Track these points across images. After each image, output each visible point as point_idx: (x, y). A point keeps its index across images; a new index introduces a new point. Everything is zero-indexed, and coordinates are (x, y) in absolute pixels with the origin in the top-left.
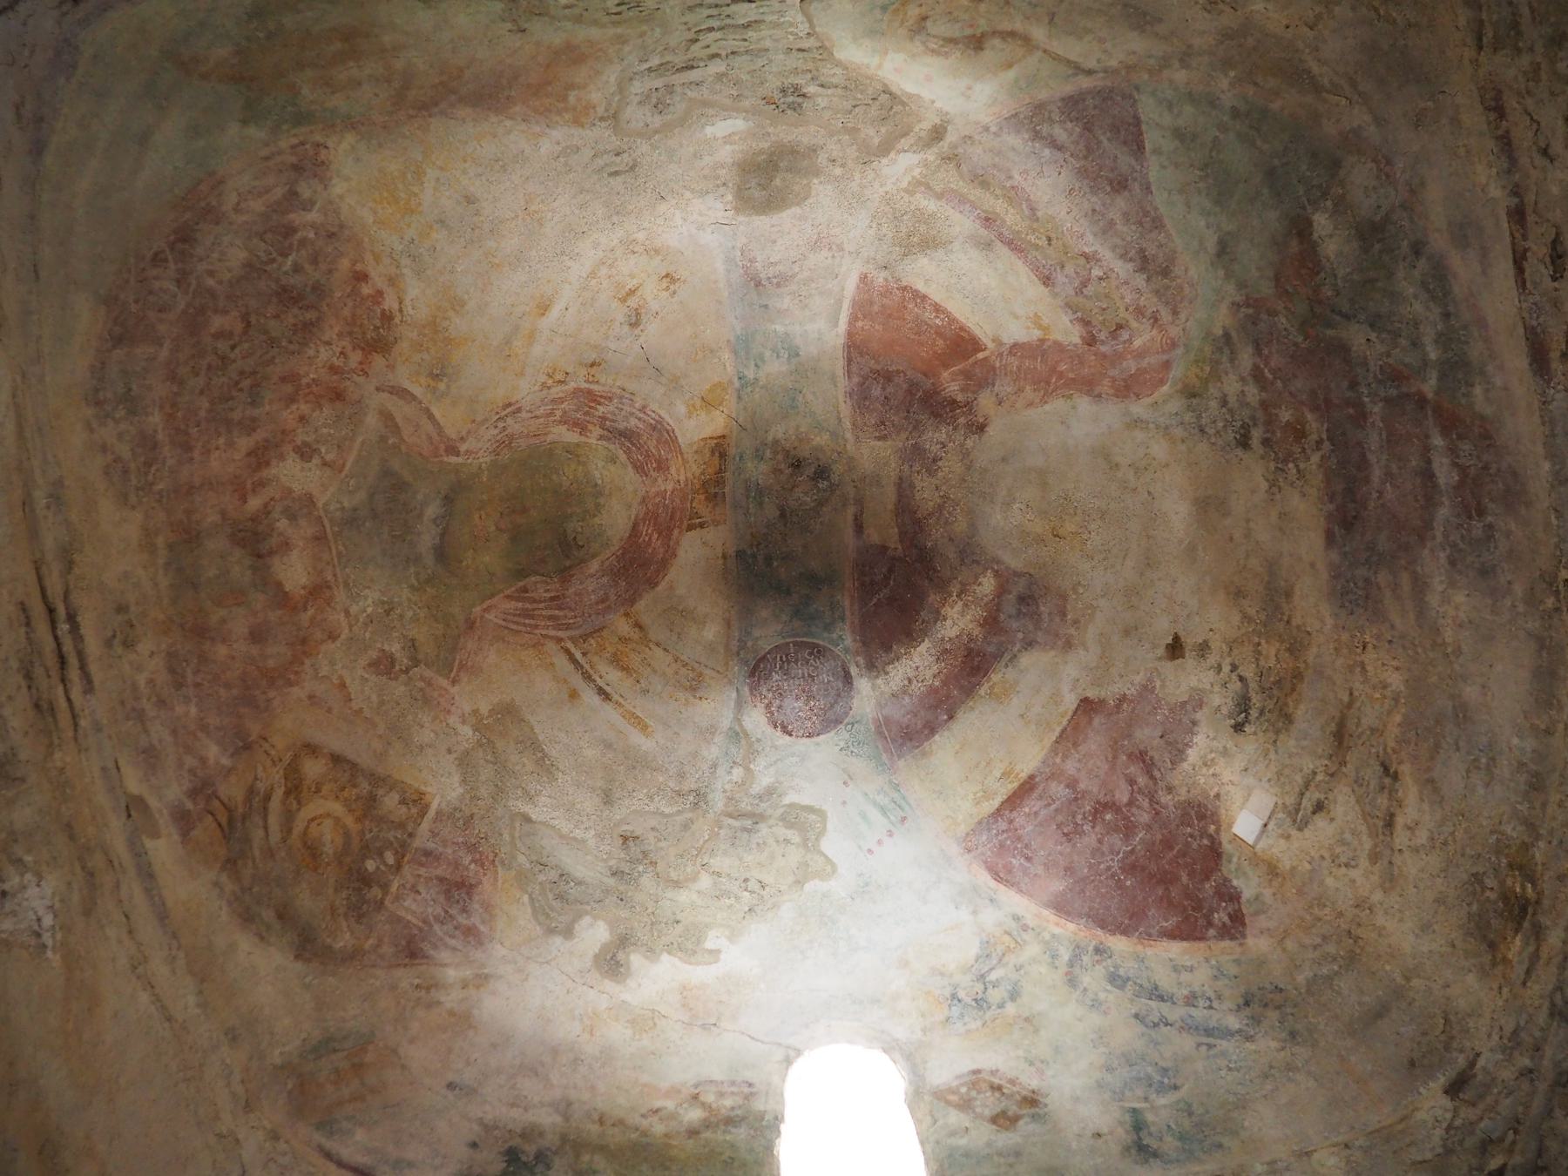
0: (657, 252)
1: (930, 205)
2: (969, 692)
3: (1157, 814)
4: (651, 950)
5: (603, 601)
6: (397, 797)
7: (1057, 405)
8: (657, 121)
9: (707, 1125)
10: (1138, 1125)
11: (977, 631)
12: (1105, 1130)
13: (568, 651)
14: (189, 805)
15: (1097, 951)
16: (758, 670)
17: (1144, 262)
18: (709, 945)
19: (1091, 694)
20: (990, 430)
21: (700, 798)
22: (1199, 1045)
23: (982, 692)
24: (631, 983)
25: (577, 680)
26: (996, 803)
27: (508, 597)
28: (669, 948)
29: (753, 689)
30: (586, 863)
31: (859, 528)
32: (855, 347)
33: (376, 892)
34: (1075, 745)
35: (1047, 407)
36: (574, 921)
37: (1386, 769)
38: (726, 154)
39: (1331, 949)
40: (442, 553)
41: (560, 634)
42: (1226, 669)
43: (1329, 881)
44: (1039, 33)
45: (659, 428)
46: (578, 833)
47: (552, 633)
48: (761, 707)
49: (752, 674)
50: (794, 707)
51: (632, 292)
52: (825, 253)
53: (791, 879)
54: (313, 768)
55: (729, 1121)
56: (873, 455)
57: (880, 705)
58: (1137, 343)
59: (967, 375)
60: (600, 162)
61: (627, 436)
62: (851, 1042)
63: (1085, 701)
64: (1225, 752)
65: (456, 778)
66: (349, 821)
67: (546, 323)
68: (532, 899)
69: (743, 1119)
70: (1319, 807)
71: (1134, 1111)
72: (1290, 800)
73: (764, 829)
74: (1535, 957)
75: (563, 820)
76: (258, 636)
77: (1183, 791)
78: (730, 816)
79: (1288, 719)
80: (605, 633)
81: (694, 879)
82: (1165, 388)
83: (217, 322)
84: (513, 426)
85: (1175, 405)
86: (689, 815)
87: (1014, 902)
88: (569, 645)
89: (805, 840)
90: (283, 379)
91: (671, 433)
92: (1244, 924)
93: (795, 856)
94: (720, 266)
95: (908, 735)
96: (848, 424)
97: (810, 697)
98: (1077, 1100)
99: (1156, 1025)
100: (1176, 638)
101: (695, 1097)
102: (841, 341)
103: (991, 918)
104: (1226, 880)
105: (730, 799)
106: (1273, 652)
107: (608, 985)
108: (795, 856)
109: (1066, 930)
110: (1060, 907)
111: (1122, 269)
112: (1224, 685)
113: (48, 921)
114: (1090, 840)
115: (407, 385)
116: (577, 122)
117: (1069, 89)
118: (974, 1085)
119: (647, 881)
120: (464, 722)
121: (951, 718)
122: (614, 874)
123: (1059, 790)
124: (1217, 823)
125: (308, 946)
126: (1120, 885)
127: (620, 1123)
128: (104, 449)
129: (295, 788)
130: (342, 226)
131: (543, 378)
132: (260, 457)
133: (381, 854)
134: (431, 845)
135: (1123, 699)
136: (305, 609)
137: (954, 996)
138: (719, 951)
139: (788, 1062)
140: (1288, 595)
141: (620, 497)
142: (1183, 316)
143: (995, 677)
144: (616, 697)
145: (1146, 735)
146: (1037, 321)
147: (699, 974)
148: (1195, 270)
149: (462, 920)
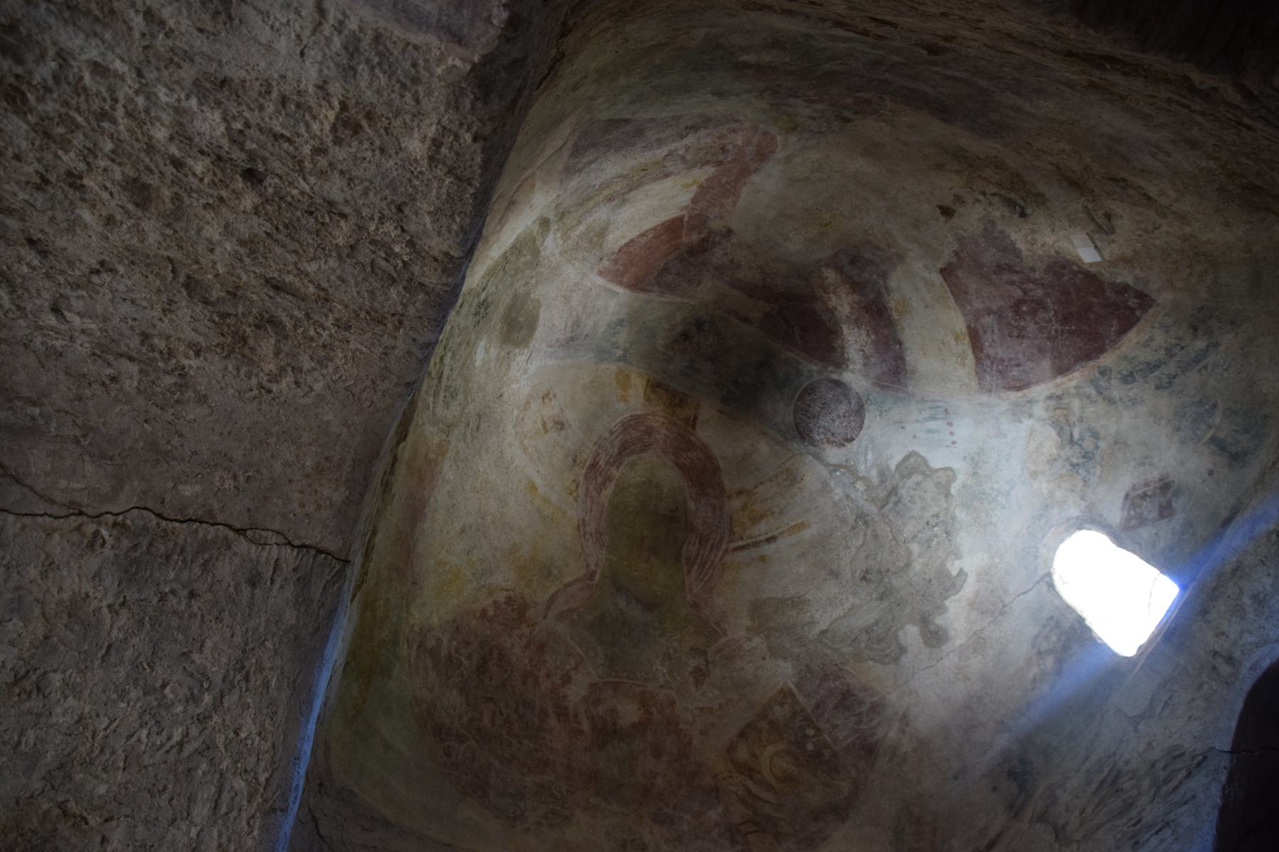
0: (528, 402)
1: (582, 228)
2: (891, 324)
3: (1042, 285)
4: (939, 608)
5: (715, 508)
6: (777, 708)
7: (745, 192)
8: (460, 397)
10: (1219, 445)
11: (856, 297)
12: (1211, 466)
13: (736, 549)
16: (802, 433)
17: (694, 128)
18: (954, 572)
21: (862, 517)
22: (1199, 371)
24: (952, 633)
25: (755, 552)
26: (971, 356)
27: (689, 572)
28: (944, 597)
29: (813, 443)
30: (869, 614)
31: (746, 320)
32: (637, 285)
33: (827, 752)
34: (966, 293)
35: (743, 196)
38: (493, 352)
40: (649, 607)
41: (723, 547)
42: (981, 198)
43: (1157, 242)
44: (527, 173)
45: (627, 426)
47: (721, 553)
50: (838, 426)
51: (544, 424)
52: (574, 295)
53: (942, 497)
54: (742, 754)
56: (705, 291)
57: (866, 376)
58: (740, 143)
59: (692, 228)
60: (469, 436)
61: (624, 448)
62: (1062, 541)
64: (1033, 232)
65: (781, 663)
67: (541, 490)
68: (873, 659)
70: (1108, 216)
72: (1092, 226)
73: (903, 492)
75: (835, 610)
76: (657, 753)
77: (1039, 264)
79: (1039, 195)
81: (910, 553)
82: (779, 138)
83: (486, 721)
84: (591, 528)
85: (793, 139)
86: (869, 531)
87: (1040, 391)
88: (733, 545)
90: (524, 683)
91: (632, 418)
92: (1147, 296)
93: (929, 485)
94: (551, 362)
95: (895, 372)
96: (679, 299)
98: (1182, 463)
99: (1170, 383)
100: (941, 208)
101: (1039, 653)
102: (628, 292)
103: (1039, 410)
104: (1113, 284)
105: (873, 500)
107: (946, 648)
108: (929, 485)
109: (1074, 379)
110: (1061, 370)
111: (690, 140)
112: (991, 204)
114: (1032, 327)
115: (547, 597)
116: (444, 454)
117: (566, 153)
118: (1134, 506)
119: (896, 582)
120: (751, 640)
121: (900, 343)
122: (882, 599)
123: (989, 320)
124: (1073, 263)
125: (839, 811)
126: (1073, 333)
128: (539, 824)
129: (748, 770)
130: (454, 621)
131: (571, 498)
132: (562, 713)
133: (806, 736)
134: (813, 702)
135: (956, 254)
136: (651, 714)
137: (1073, 465)
138: (961, 570)
139: (1051, 585)
141: (657, 469)
142: (742, 118)
143: (892, 304)
144: (776, 533)
145: (990, 256)
146: (687, 186)
147: (969, 588)
148: (719, 108)
149: (864, 708)
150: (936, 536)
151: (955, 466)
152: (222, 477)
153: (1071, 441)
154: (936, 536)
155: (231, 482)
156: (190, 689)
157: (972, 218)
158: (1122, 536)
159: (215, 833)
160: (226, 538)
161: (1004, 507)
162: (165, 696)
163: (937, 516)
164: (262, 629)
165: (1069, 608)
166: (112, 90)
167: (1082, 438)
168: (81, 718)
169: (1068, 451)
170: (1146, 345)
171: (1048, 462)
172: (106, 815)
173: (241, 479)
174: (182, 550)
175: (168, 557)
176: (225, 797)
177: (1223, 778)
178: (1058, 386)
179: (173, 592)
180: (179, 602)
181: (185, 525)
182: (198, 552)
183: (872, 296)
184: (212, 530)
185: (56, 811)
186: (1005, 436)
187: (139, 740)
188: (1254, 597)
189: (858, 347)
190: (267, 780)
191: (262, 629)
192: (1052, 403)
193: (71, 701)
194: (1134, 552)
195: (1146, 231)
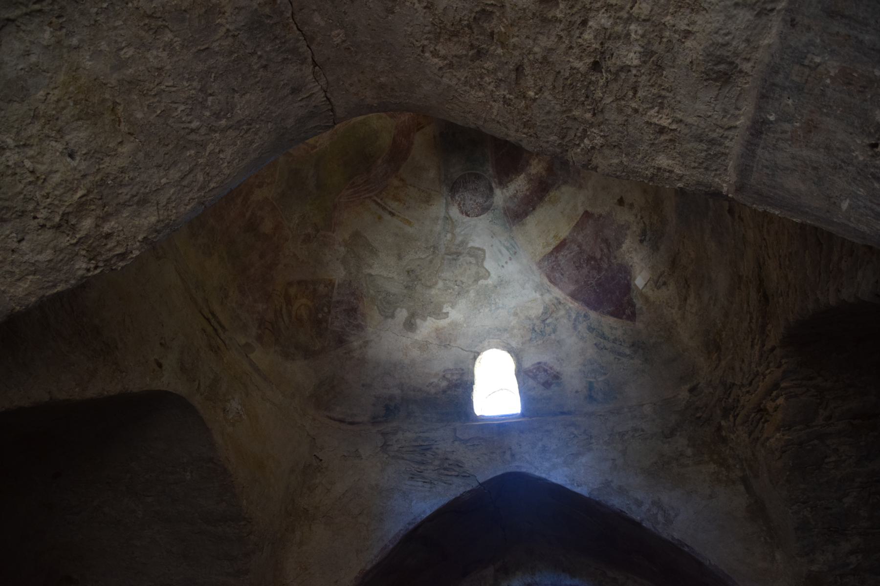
2: (541, 199)
9: (449, 388)
10: (590, 387)
11: (544, 173)
13: (375, 201)
14: (260, 332)
16: (454, 188)
18: (444, 311)
19: (589, 209)
24: (418, 332)
26: (551, 248)
28: (430, 315)
29: (453, 197)
30: (395, 288)
42: (639, 217)
46: (390, 275)
47: (367, 195)
48: (456, 205)
49: (451, 191)
54: (293, 291)
55: (456, 386)
62: (497, 348)
63: (586, 212)
64: (636, 250)
70: (665, 284)
71: (591, 383)
73: (461, 258)
75: (384, 272)
78: (447, 254)
81: (436, 283)
87: (557, 293)
88: (375, 198)
89: (477, 262)
95: (517, 215)
100: (622, 198)
101: (444, 376)
103: (547, 297)
107: (410, 334)
109: (573, 305)
110: (574, 296)
112: (638, 223)
113: (240, 408)
114: (585, 271)
118: (538, 369)
119: (419, 288)
121: (534, 209)
127: (420, 390)
135: (600, 216)
137: (533, 329)
139: (475, 358)
143: (552, 194)
144: (397, 213)
147: (443, 323)
151: (492, 275)
152: (339, 35)
153: (544, 321)
155: (339, 41)
156: (221, 110)
157: (624, 216)
158: (521, 373)
159: (172, 191)
160: (306, 58)
162: (206, 100)
163: (463, 283)
164: (274, 115)
167: (548, 325)
168: (159, 69)
169: (537, 322)
170: (611, 328)
172: (131, 131)
173: (345, 45)
174: (284, 43)
175: (276, 38)
176: (190, 178)
177: (468, 489)
178: (565, 299)
180: (256, 63)
181: (298, 32)
183: (550, 182)
184: (306, 48)
185: (110, 104)
186: (524, 288)
187: (176, 109)
188: (544, 446)
189: (518, 188)
190: (213, 188)
191: (274, 115)
192: (555, 301)
193: (164, 55)
195: (667, 303)
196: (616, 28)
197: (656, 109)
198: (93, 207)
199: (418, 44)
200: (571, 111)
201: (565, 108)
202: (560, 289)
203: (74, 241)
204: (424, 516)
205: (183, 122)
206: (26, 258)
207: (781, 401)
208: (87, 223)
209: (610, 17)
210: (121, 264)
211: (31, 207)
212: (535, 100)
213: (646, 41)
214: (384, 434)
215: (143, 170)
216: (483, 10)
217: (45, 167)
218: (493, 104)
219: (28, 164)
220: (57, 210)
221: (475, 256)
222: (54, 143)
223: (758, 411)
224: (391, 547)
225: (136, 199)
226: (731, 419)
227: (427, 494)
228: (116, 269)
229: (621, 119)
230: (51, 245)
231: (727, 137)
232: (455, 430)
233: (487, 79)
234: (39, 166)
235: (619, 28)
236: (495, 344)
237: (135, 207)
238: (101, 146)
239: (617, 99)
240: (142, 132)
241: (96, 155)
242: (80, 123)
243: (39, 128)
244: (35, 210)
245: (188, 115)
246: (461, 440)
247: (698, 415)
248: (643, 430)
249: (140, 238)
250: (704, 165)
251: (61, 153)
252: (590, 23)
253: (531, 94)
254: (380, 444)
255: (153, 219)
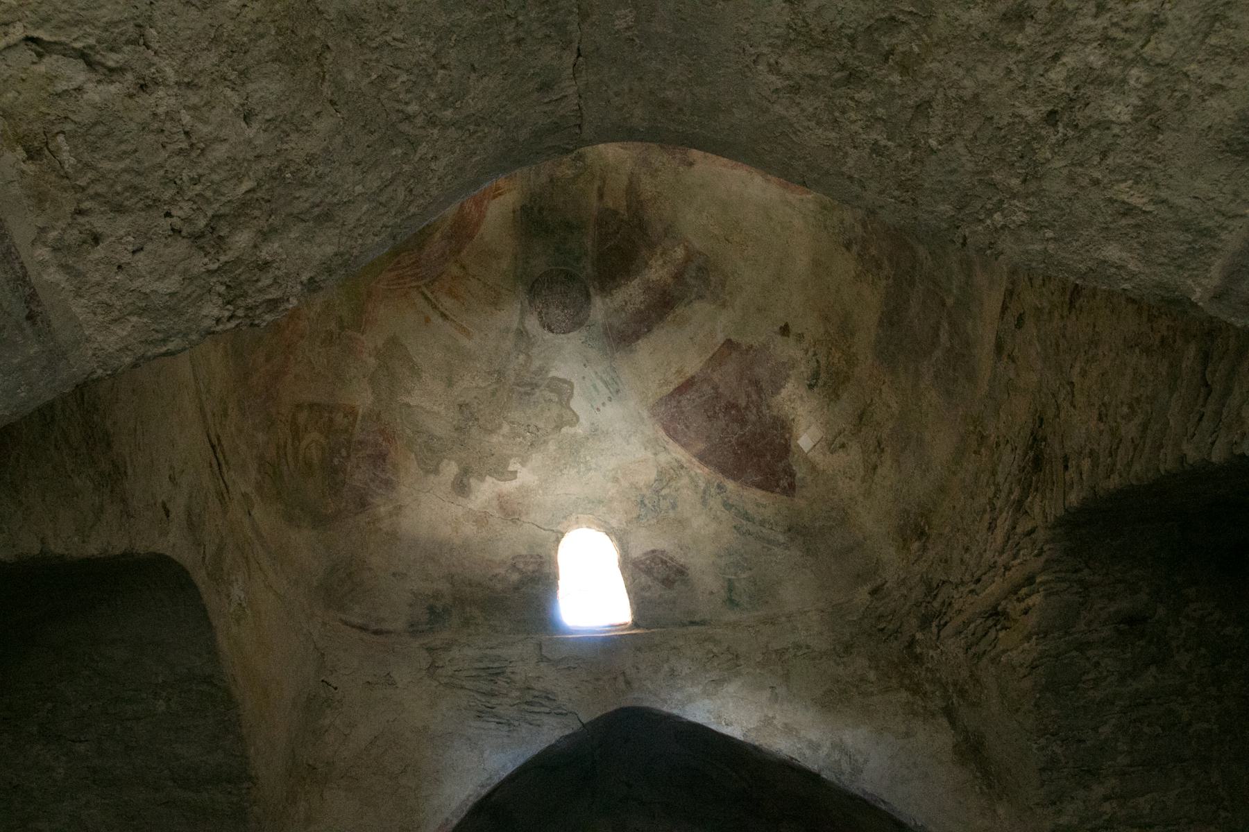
2: (661, 318)
9: (522, 583)
11: (670, 280)
15: (719, 487)
18: (511, 468)
19: (734, 338)
20: (696, 167)
23: (669, 318)
27: (390, 271)
30: (440, 424)
31: (601, 196)
36: (438, 464)
37: (879, 444)
39: (834, 514)
42: (810, 353)
43: (840, 483)
47: (414, 284)
49: (530, 291)
50: (556, 313)
54: (302, 417)
63: (729, 340)
64: (801, 398)
65: (369, 392)
66: (322, 440)
69: (539, 579)
70: (843, 446)
72: (830, 437)
74: (919, 558)
75: (429, 403)
79: (838, 397)
80: (444, 276)
81: (500, 426)
87: (678, 453)
88: (424, 289)
93: (555, 410)
95: (622, 338)
97: (565, 307)
100: (787, 325)
101: (514, 566)
104: (790, 466)
106: (837, 355)
108: (555, 410)
109: (702, 472)
110: (702, 458)
118: (653, 560)
119: (474, 431)
123: (707, 389)
129: (296, 434)
137: (642, 501)
139: (558, 541)
140: (852, 335)
143: (679, 310)
145: (761, 372)
147: (508, 486)
150: (524, 438)
154: (524, 438)
156: (451, 94)
157: (787, 350)
159: (365, 208)
161: (578, 472)
165: (553, 562)
166: (1137, 30)
167: (665, 498)
169: (648, 493)
170: (758, 505)
171: (632, 484)
172: (335, 98)
177: (567, 732)
179: (519, 24)
180: (510, 34)
182: (555, 25)
190: (414, 215)
194: (625, 579)
196: (1109, 71)
197: (1130, 182)
198: (257, 213)
199: (752, 51)
200: (988, 172)
201: (980, 168)
202: (684, 446)
203: (215, 266)
204: (504, 774)
205: (398, 101)
206: (137, 284)
207: (1036, 599)
208: (242, 239)
209: (1104, 54)
210: (268, 317)
211: (167, 195)
212: (933, 151)
213: (1151, 91)
214: (430, 650)
215: (337, 164)
216: (892, 18)
217: (210, 128)
218: (851, 151)
219: (186, 118)
220: (205, 207)
221: (559, 393)
222: (229, 92)
223: (991, 615)
224: (455, 822)
225: (316, 211)
226: (934, 630)
227: (506, 740)
228: (258, 325)
229: (1068, 191)
230: (180, 267)
231: (1226, 228)
232: (540, 646)
233: (853, 115)
234: (200, 126)
235: (1116, 71)
236: (589, 522)
237: (311, 224)
238: (293, 113)
239: (1073, 164)
240: (347, 103)
241: (284, 126)
242: (276, 66)
243: (215, 60)
244: (173, 201)
245: (408, 91)
246: (549, 660)
247: (882, 626)
248: (808, 647)
249: (304, 278)
250: (1179, 262)
251: (237, 110)
252: (1064, 60)
253: (933, 143)
254: (425, 665)
255: (329, 250)
